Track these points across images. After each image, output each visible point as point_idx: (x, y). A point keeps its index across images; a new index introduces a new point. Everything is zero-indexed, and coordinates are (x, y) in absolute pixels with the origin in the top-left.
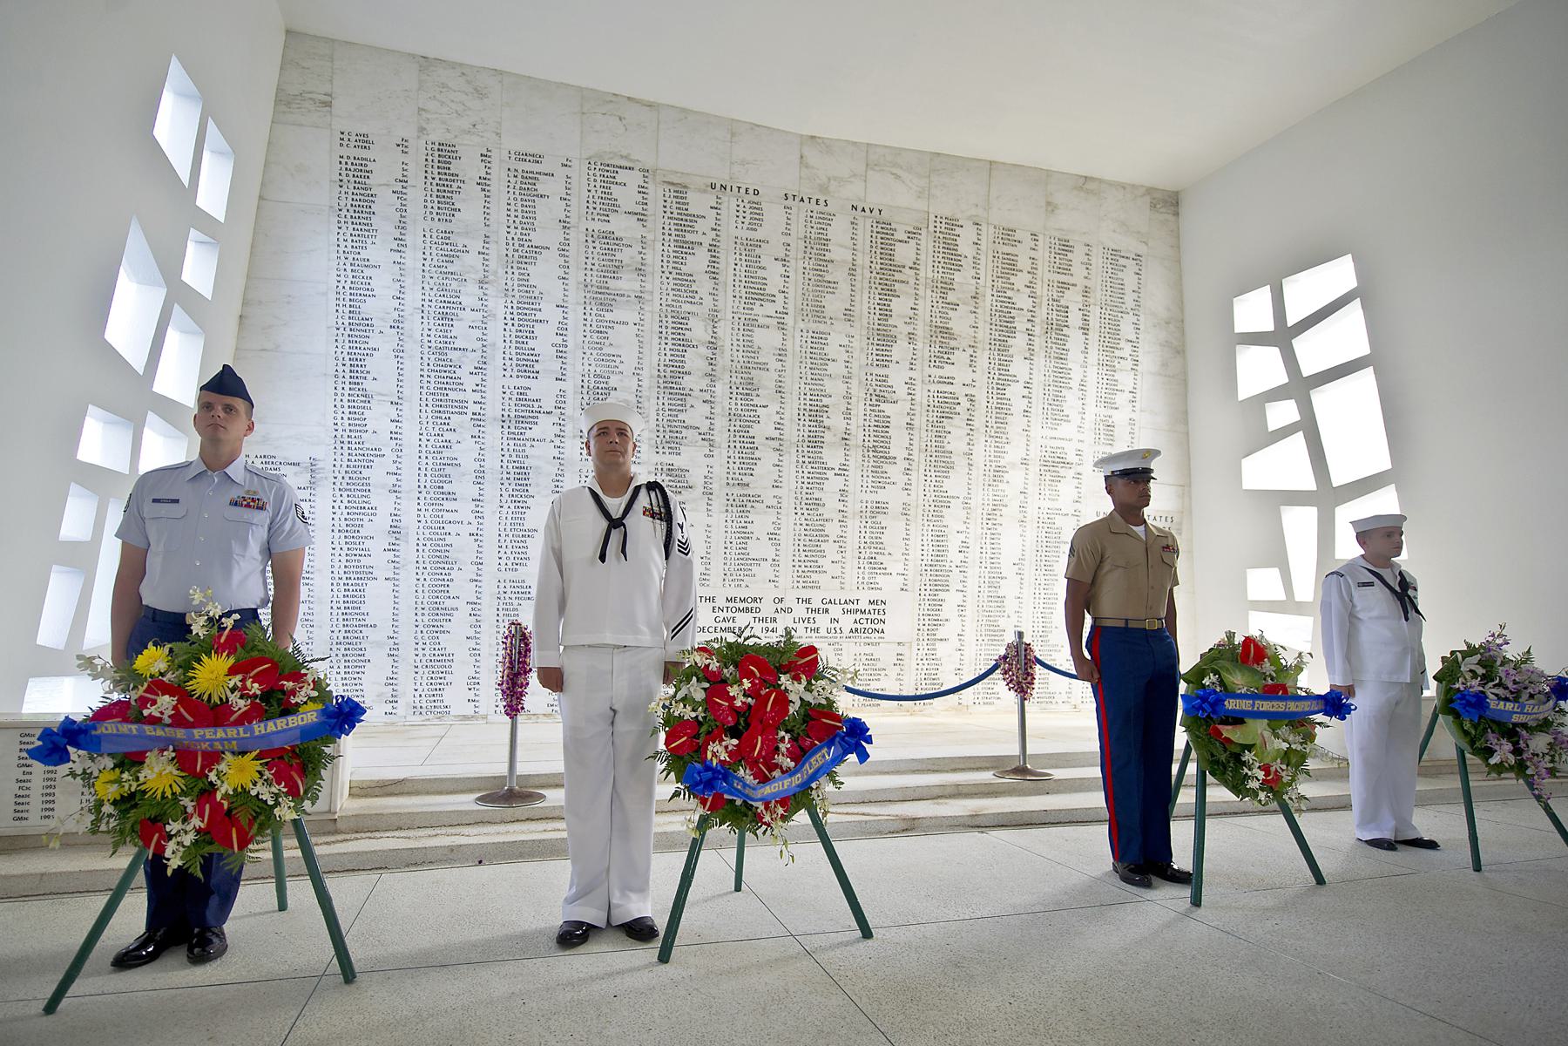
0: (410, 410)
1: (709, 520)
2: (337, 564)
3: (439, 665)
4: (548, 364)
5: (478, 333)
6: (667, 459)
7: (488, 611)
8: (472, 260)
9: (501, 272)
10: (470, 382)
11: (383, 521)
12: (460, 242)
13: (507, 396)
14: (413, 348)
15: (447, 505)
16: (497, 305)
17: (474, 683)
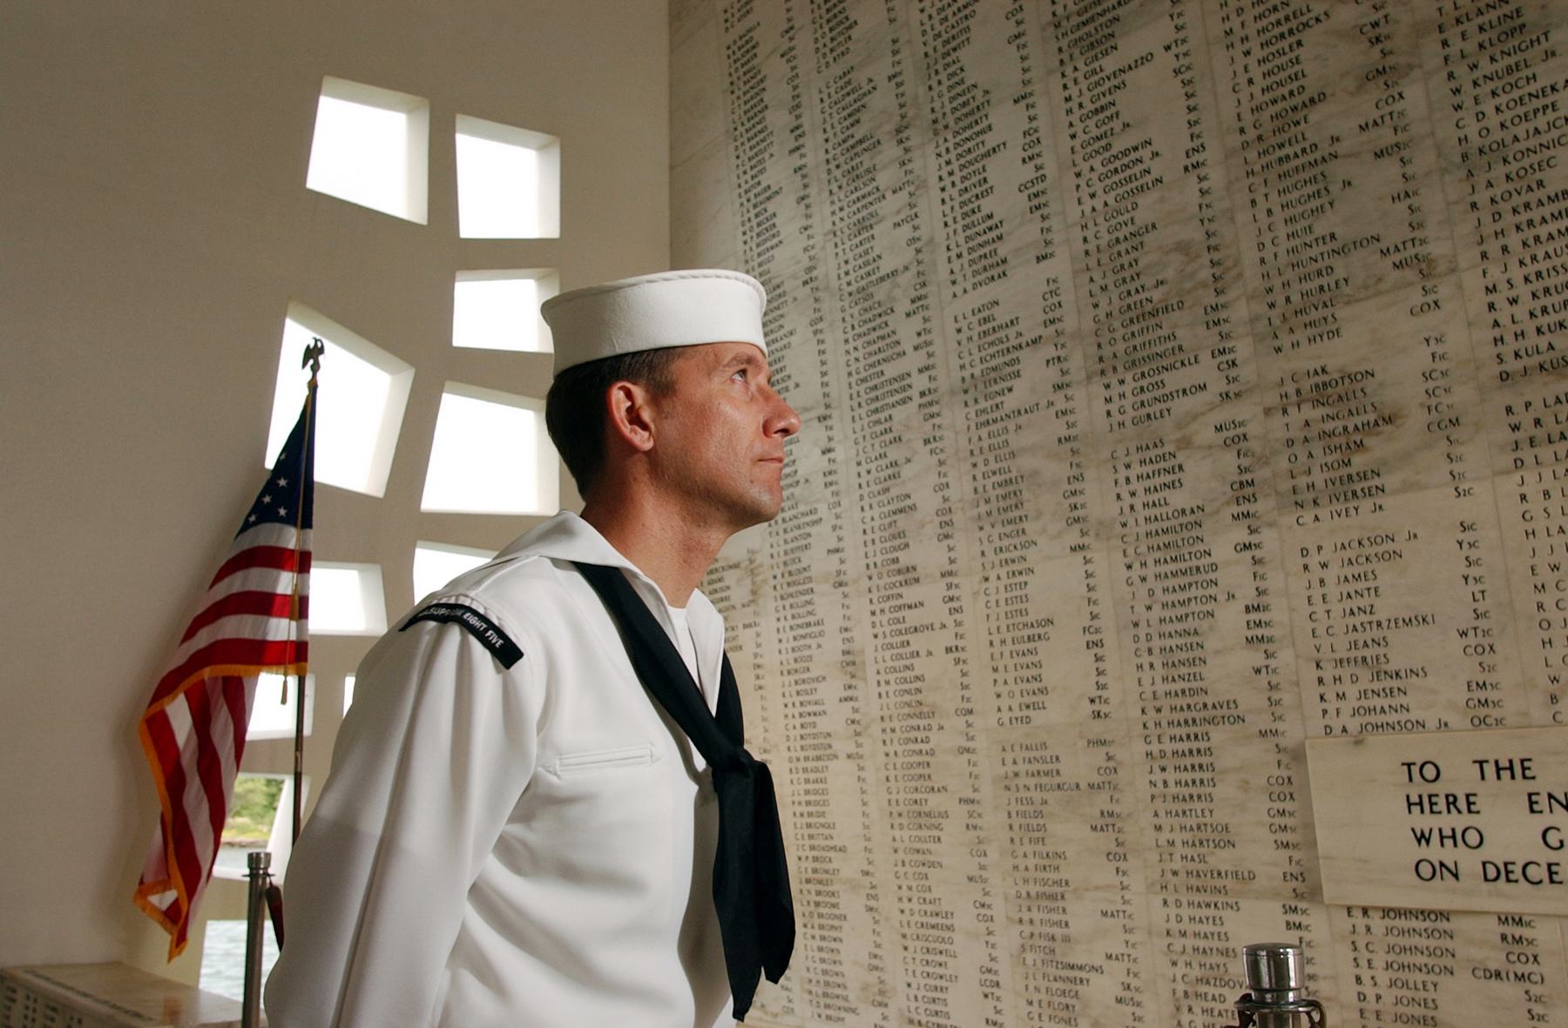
0: (841, 424)
1: (1465, 509)
2: (792, 733)
3: (934, 931)
4: (1022, 234)
5: (906, 231)
6: (1307, 358)
7: (993, 821)
8: (882, 101)
9: (922, 90)
10: (906, 332)
11: (833, 644)
12: (860, 77)
13: (963, 337)
14: (831, 306)
15: (911, 594)
16: (927, 164)
17: (990, 985)
